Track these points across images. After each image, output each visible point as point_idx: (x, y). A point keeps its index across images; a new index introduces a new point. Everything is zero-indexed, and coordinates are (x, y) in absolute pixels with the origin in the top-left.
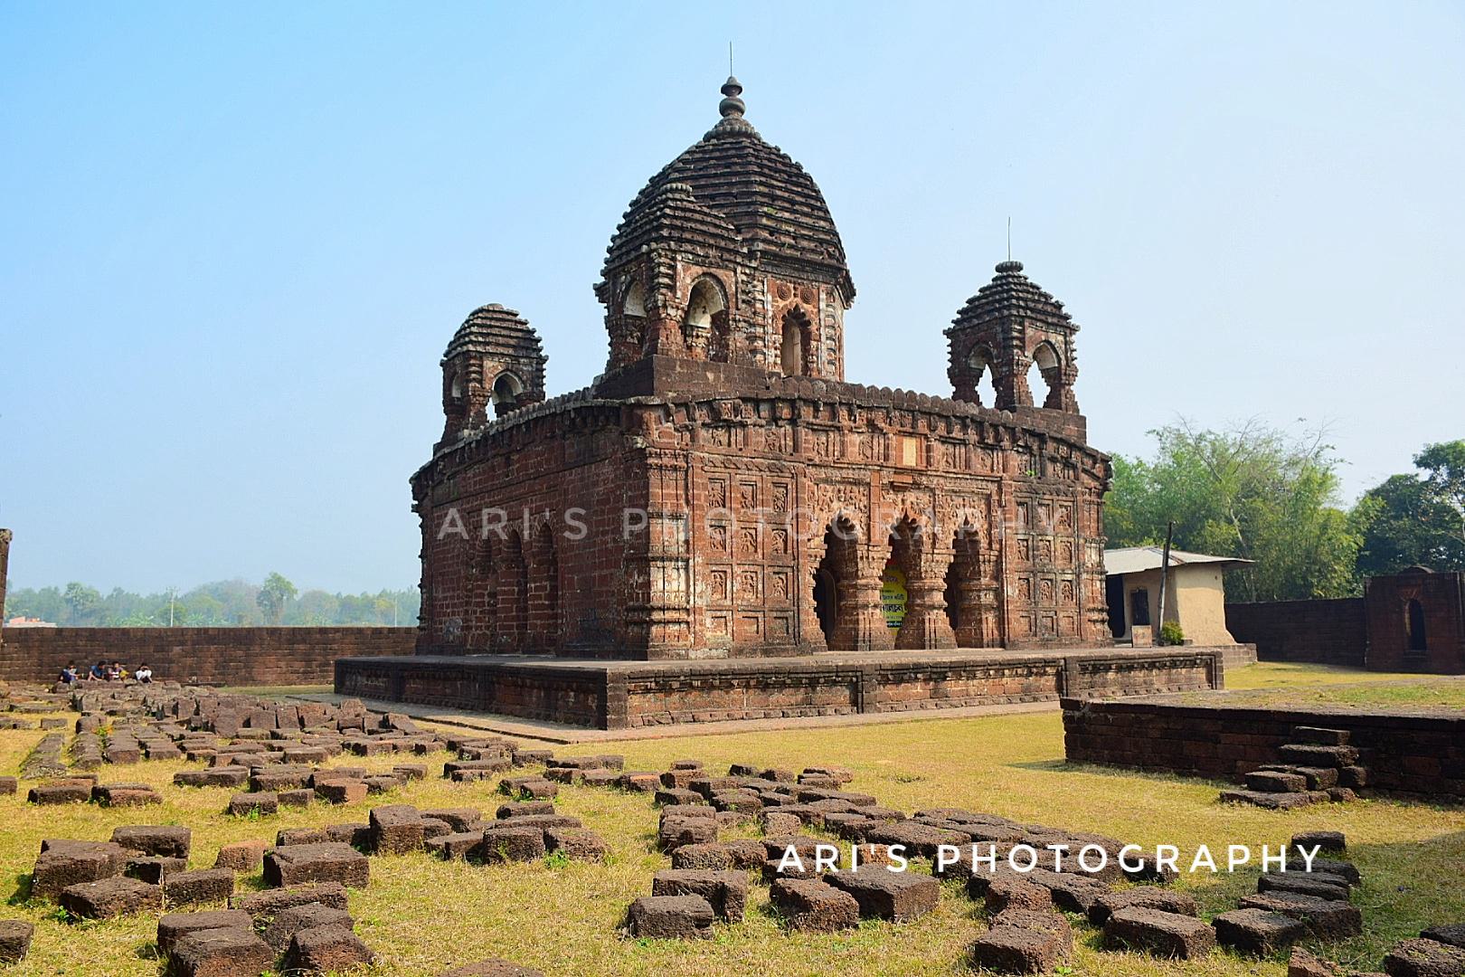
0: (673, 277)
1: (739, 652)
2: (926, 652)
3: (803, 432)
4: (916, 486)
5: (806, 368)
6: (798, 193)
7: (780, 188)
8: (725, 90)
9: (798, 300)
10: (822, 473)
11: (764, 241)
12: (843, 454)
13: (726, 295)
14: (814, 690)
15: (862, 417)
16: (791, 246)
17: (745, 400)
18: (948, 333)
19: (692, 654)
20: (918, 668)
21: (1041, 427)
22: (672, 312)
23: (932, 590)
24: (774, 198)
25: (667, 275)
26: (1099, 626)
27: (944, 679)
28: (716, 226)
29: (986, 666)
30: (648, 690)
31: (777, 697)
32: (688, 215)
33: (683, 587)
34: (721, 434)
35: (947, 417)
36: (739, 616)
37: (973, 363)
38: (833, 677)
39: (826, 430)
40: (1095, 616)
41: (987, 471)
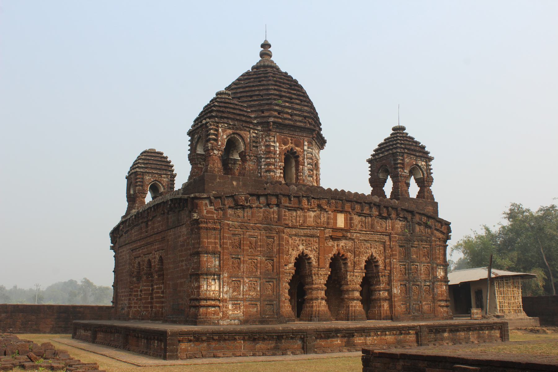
0: (216, 135)
2: (349, 322)
3: (283, 210)
4: (345, 238)
5: (297, 179)
6: (294, 94)
7: (285, 92)
9: (293, 145)
10: (294, 231)
11: (275, 117)
12: (304, 221)
13: (244, 143)
14: (281, 343)
15: (314, 202)
16: (290, 120)
18: (369, 161)
19: (221, 322)
20: (337, 331)
21: (413, 208)
22: (216, 152)
23: (353, 290)
24: (281, 96)
25: (214, 134)
26: (445, 309)
27: (353, 336)
28: (240, 110)
29: (376, 330)
30: (190, 341)
31: (260, 345)
32: (227, 105)
33: (217, 289)
34: (240, 212)
35: (361, 203)
36: (247, 303)
37: (381, 176)
38: (293, 335)
40: (443, 304)
41: (383, 230)
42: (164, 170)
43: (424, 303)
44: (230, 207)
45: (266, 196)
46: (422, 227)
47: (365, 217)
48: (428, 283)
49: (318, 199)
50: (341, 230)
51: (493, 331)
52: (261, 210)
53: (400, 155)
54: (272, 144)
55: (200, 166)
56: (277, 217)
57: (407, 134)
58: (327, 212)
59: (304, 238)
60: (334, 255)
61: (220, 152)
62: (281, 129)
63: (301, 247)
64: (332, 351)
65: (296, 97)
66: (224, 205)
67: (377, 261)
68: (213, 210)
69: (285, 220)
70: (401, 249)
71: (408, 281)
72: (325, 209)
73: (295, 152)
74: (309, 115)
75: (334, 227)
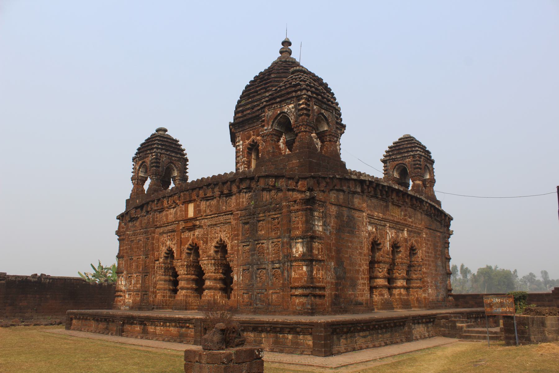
1: (132, 308)
8: (283, 43)
9: (254, 137)
10: (161, 230)
19: (122, 308)
29: (160, 319)
43: (271, 291)
44: (129, 221)
46: (273, 192)
48: (277, 265)
50: (191, 219)
51: (301, 337)
52: (146, 218)
54: (238, 144)
59: (169, 234)
60: (190, 245)
63: (168, 243)
64: (132, 336)
67: (226, 246)
69: (157, 221)
70: (247, 226)
71: (252, 264)
73: (256, 142)
75: (185, 219)
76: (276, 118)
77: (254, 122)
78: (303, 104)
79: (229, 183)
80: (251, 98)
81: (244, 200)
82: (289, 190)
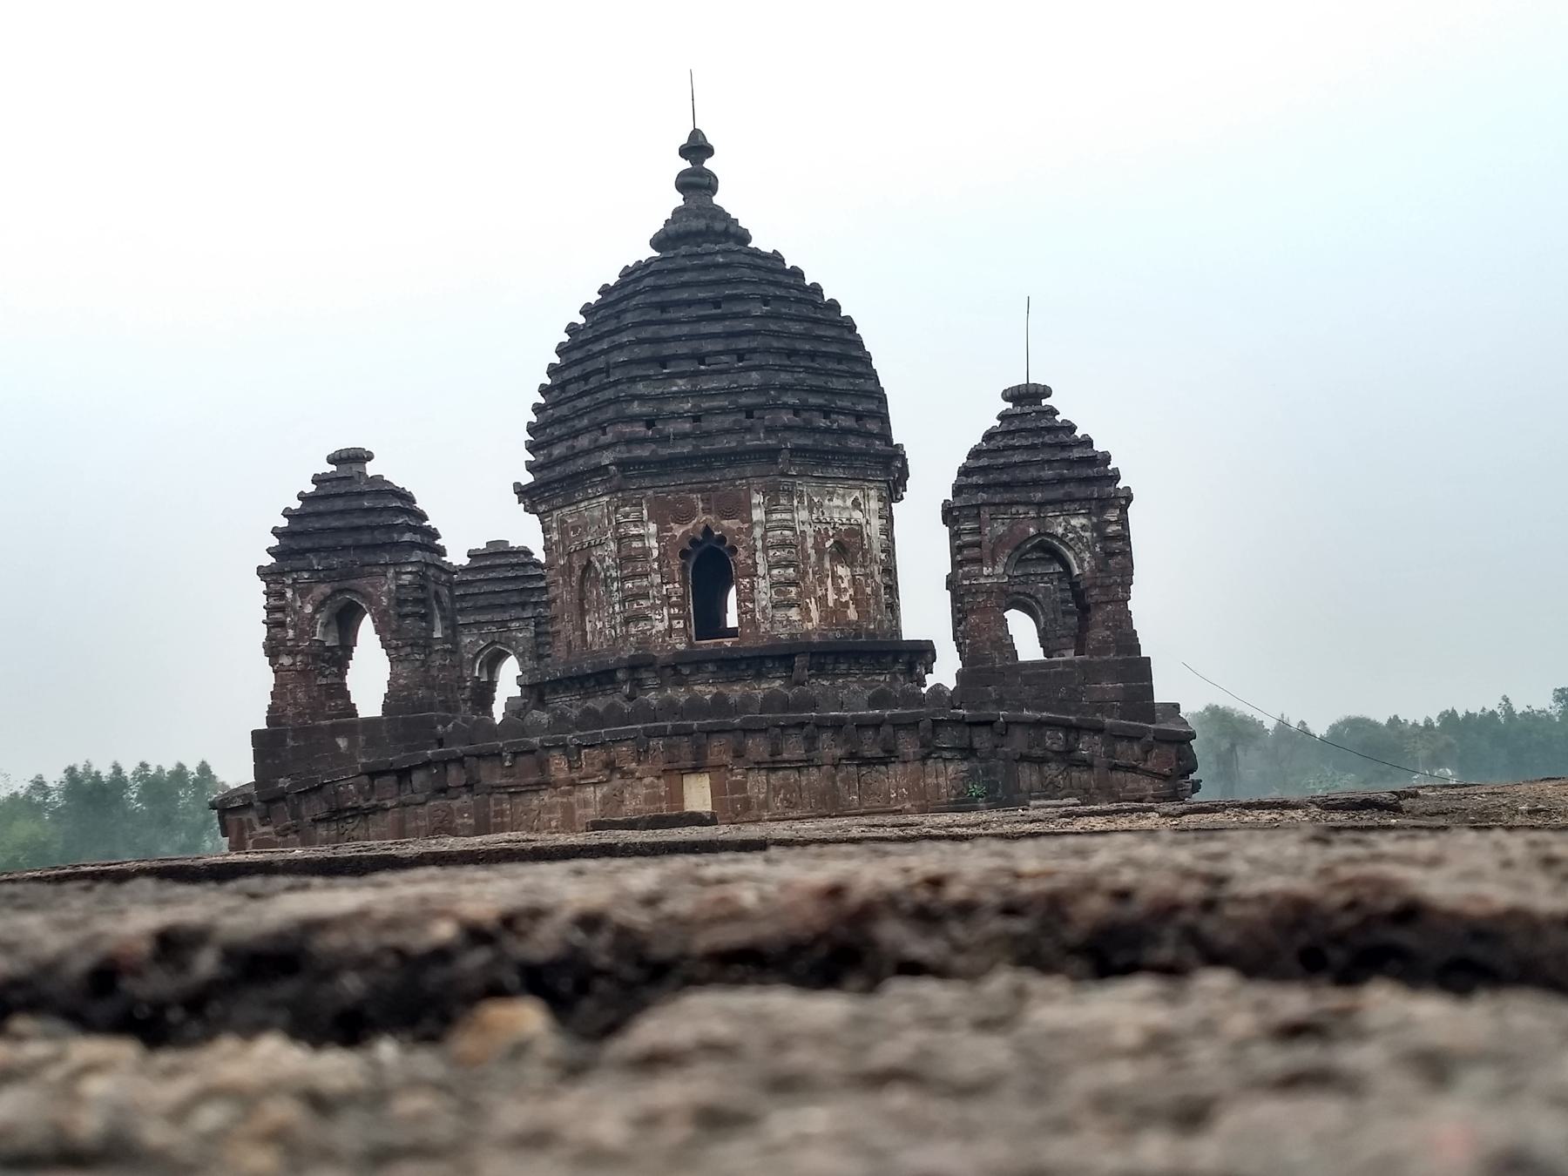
7: (677, 338)
8: (684, 152)
17: (373, 774)
24: (663, 362)
39: (537, 788)
42: (515, 605)
45: (427, 764)
47: (798, 769)
49: (603, 744)
53: (967, 518)
54: (634, 531)
55: (324, 682)
56: (472, 821)
57: (1055, 412)
58: (640, 779)
61: (299, 658)
62: (658, 475)
65: (719, 346)
66: (296, 815)
68: (273, 836)
72: (632, 773)
73: (722, 539)
74: (762, 400)
76: (1017, 548)
77: (711, 469)
78: (1116, 522)
79: (886, 730)
80: (681, 375)
81: (941, 780)
82: (1115, 768)
